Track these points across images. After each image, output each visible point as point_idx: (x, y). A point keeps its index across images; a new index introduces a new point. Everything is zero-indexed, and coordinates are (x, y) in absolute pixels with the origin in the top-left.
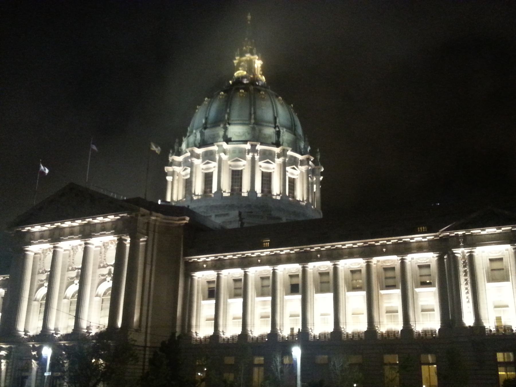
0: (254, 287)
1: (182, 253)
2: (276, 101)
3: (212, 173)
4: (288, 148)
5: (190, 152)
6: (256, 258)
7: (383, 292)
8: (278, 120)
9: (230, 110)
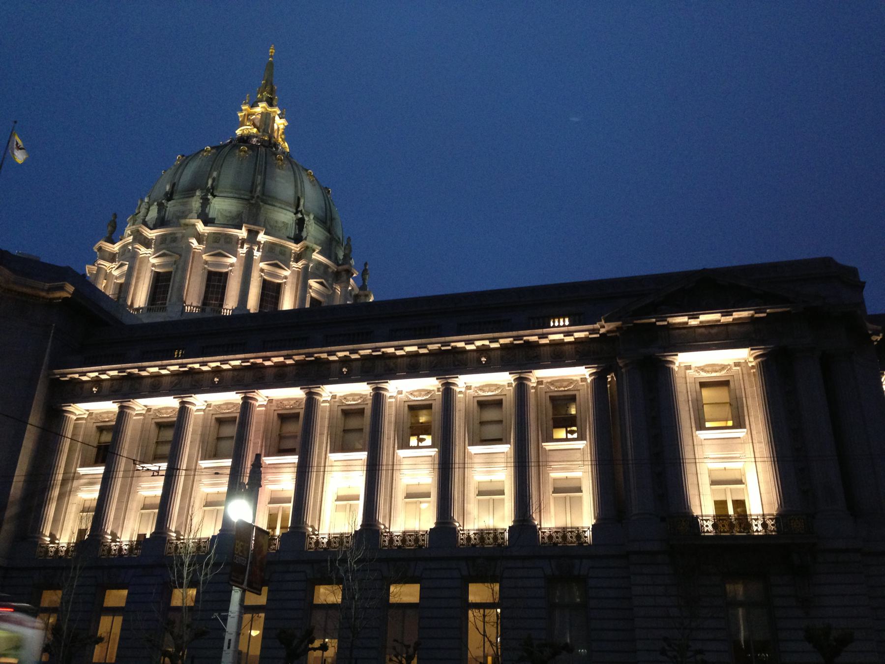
0: (198, 438)
1: (46, 358)
2: (304, 174)
4: (315, 246)
6: (211, 375)
7: (474, 450)
8: (302, 203)
9: (219, 175)
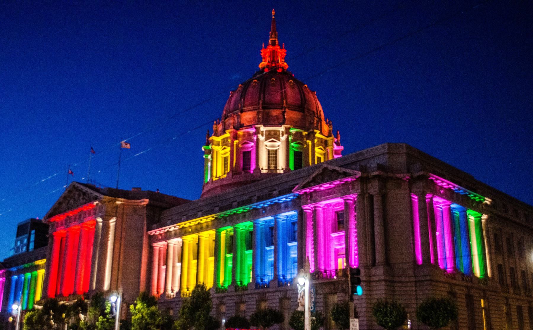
3: (249, 152)
5: (229, 133)
